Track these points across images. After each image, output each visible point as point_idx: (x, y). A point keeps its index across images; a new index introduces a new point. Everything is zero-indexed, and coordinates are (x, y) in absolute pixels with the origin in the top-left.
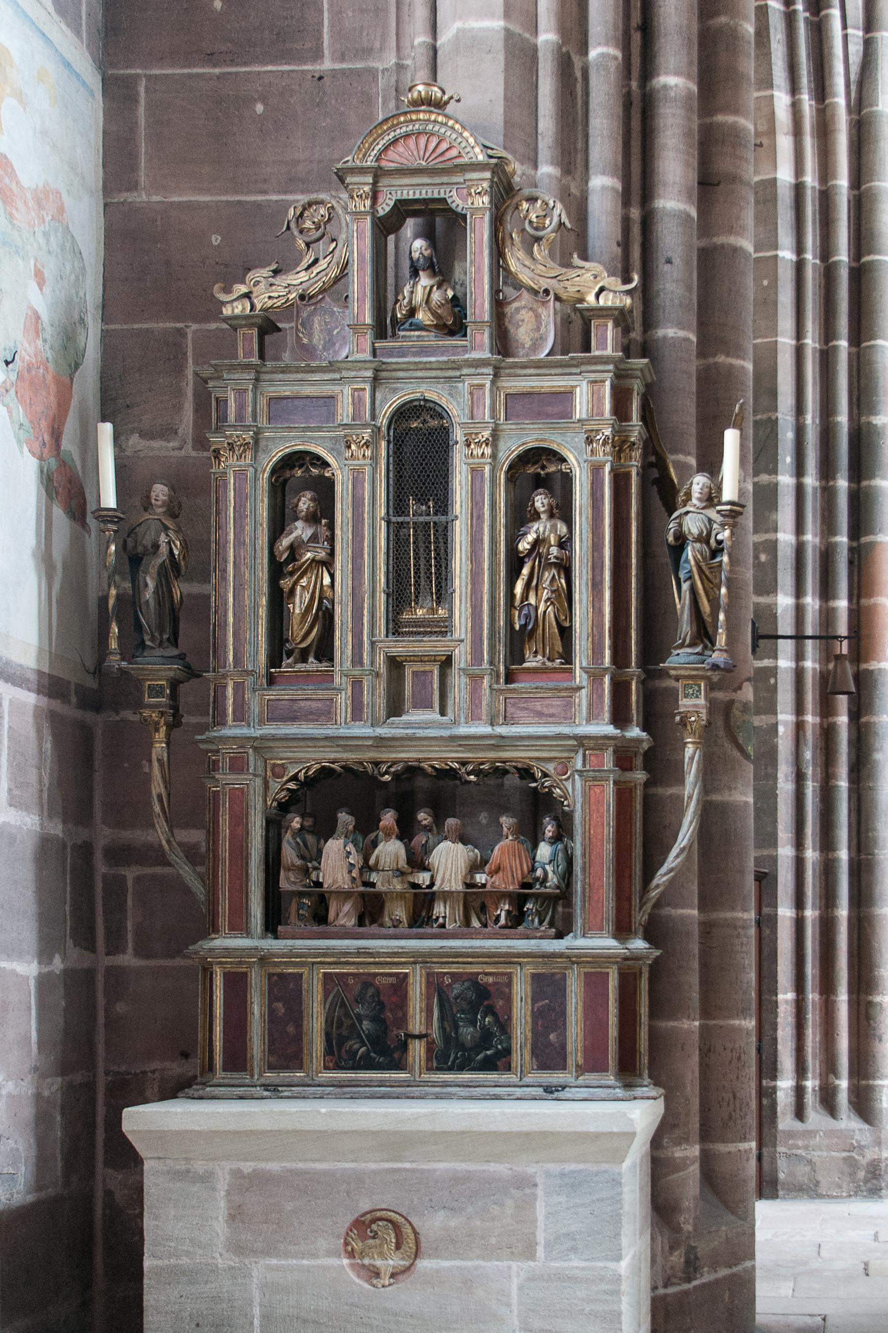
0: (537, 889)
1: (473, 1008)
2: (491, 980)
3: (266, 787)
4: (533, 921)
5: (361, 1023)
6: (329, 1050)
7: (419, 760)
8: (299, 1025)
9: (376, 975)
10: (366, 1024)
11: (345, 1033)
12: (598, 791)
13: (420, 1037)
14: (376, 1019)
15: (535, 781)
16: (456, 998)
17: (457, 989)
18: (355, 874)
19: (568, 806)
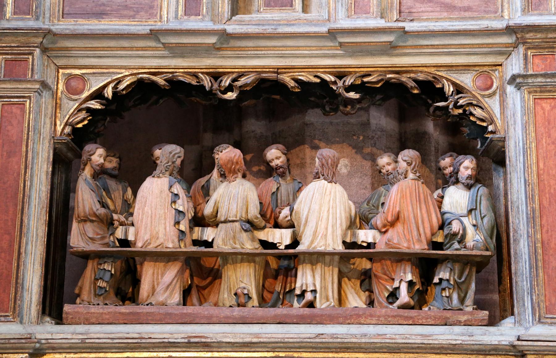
0: (454, 249)
3: (57, 106)
4: (449, 297)
7: (278, 70)
15: (446, 100)
18: (183, 226)
19: (492, 132)
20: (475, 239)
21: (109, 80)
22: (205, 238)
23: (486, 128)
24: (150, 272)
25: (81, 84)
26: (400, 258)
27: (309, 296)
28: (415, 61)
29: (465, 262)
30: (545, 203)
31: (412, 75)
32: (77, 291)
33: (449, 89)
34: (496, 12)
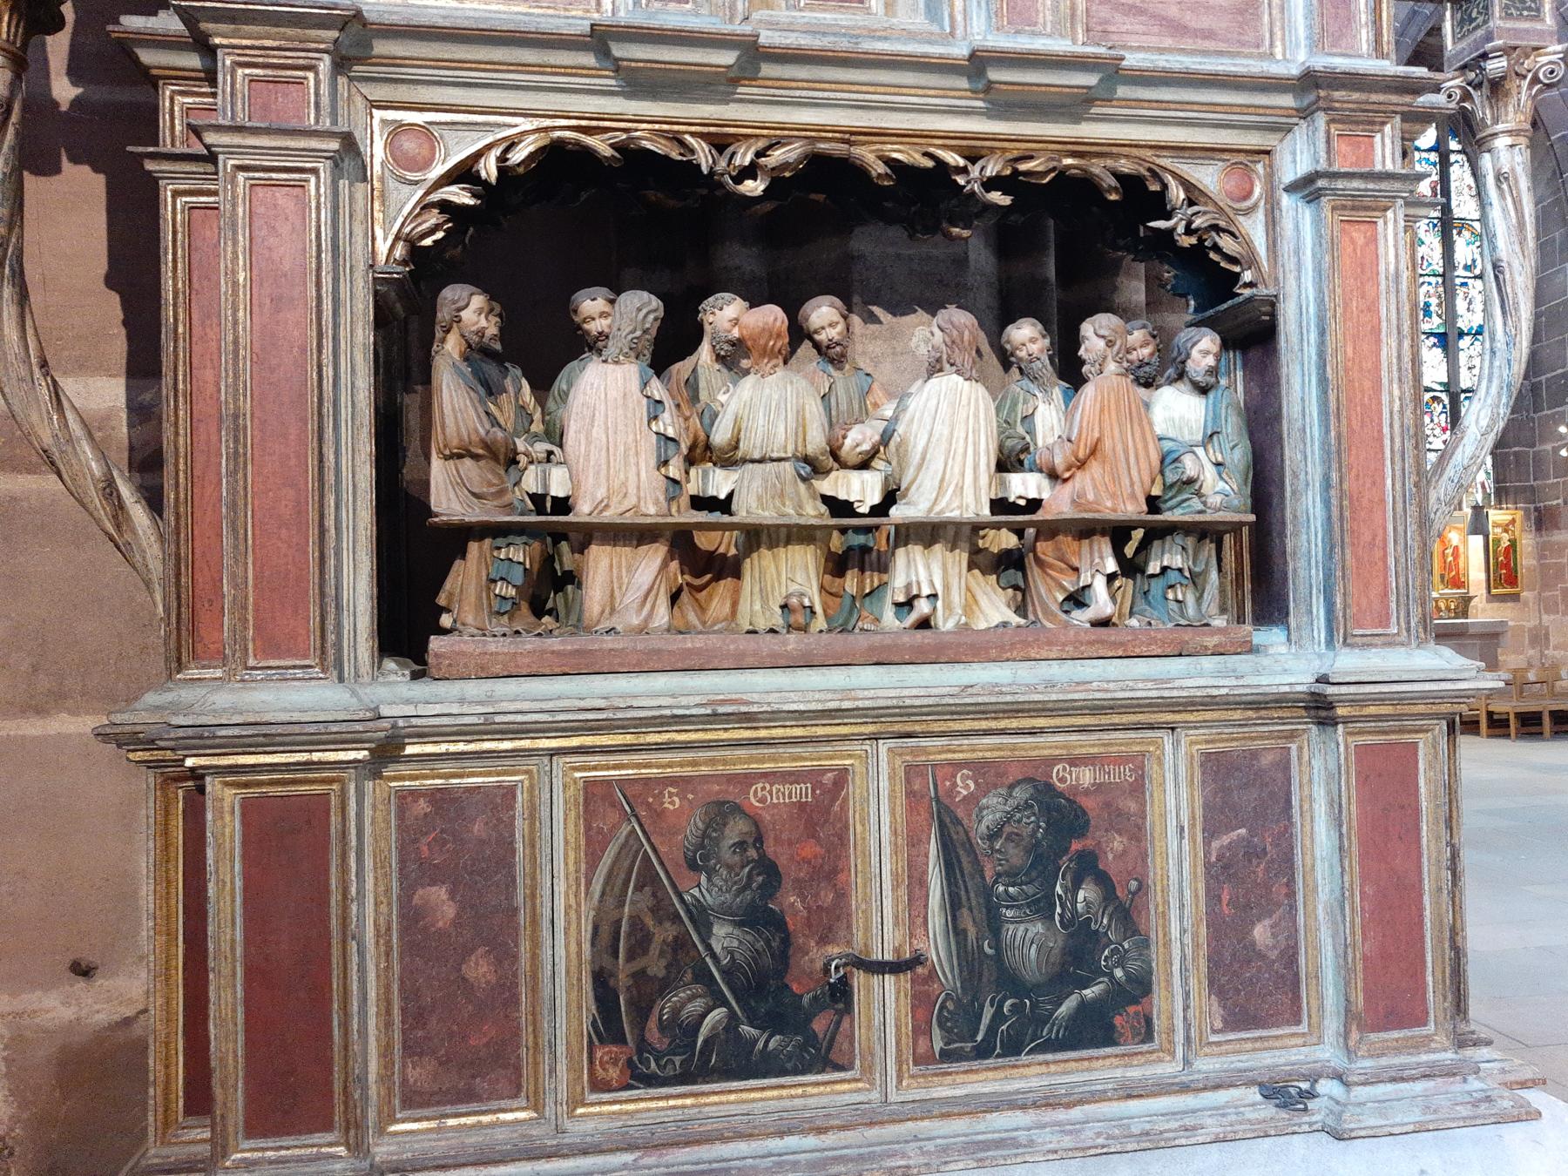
1: (1042, 863)
2: (1086, 776)
5: (705, 930)
6: (607, 1027)
7: (851, 136)
8: (504, 954)
9: (748, 779)
10: (723, 936)
11: (657, 968)
12: (1361, 240)
13: (895, 968)
14: (759, 917)
16: (992, 836)
17: (994, 807)
18: (674, 470)
19: (1251, 285)
20: (1220, 492)
21: (490, 139)
22: (711, 492)
23: (1237, 276)
24: (604, 563)
25: (426, 146)
26: (1085, 530)
27: (923, 607)
28: (1117, 134)
29: (1206, 533)
30: (1356, 425)
31: (1109, 163)
32: (442, 600)
33: (1177, 194)
34: (1258, 47)
